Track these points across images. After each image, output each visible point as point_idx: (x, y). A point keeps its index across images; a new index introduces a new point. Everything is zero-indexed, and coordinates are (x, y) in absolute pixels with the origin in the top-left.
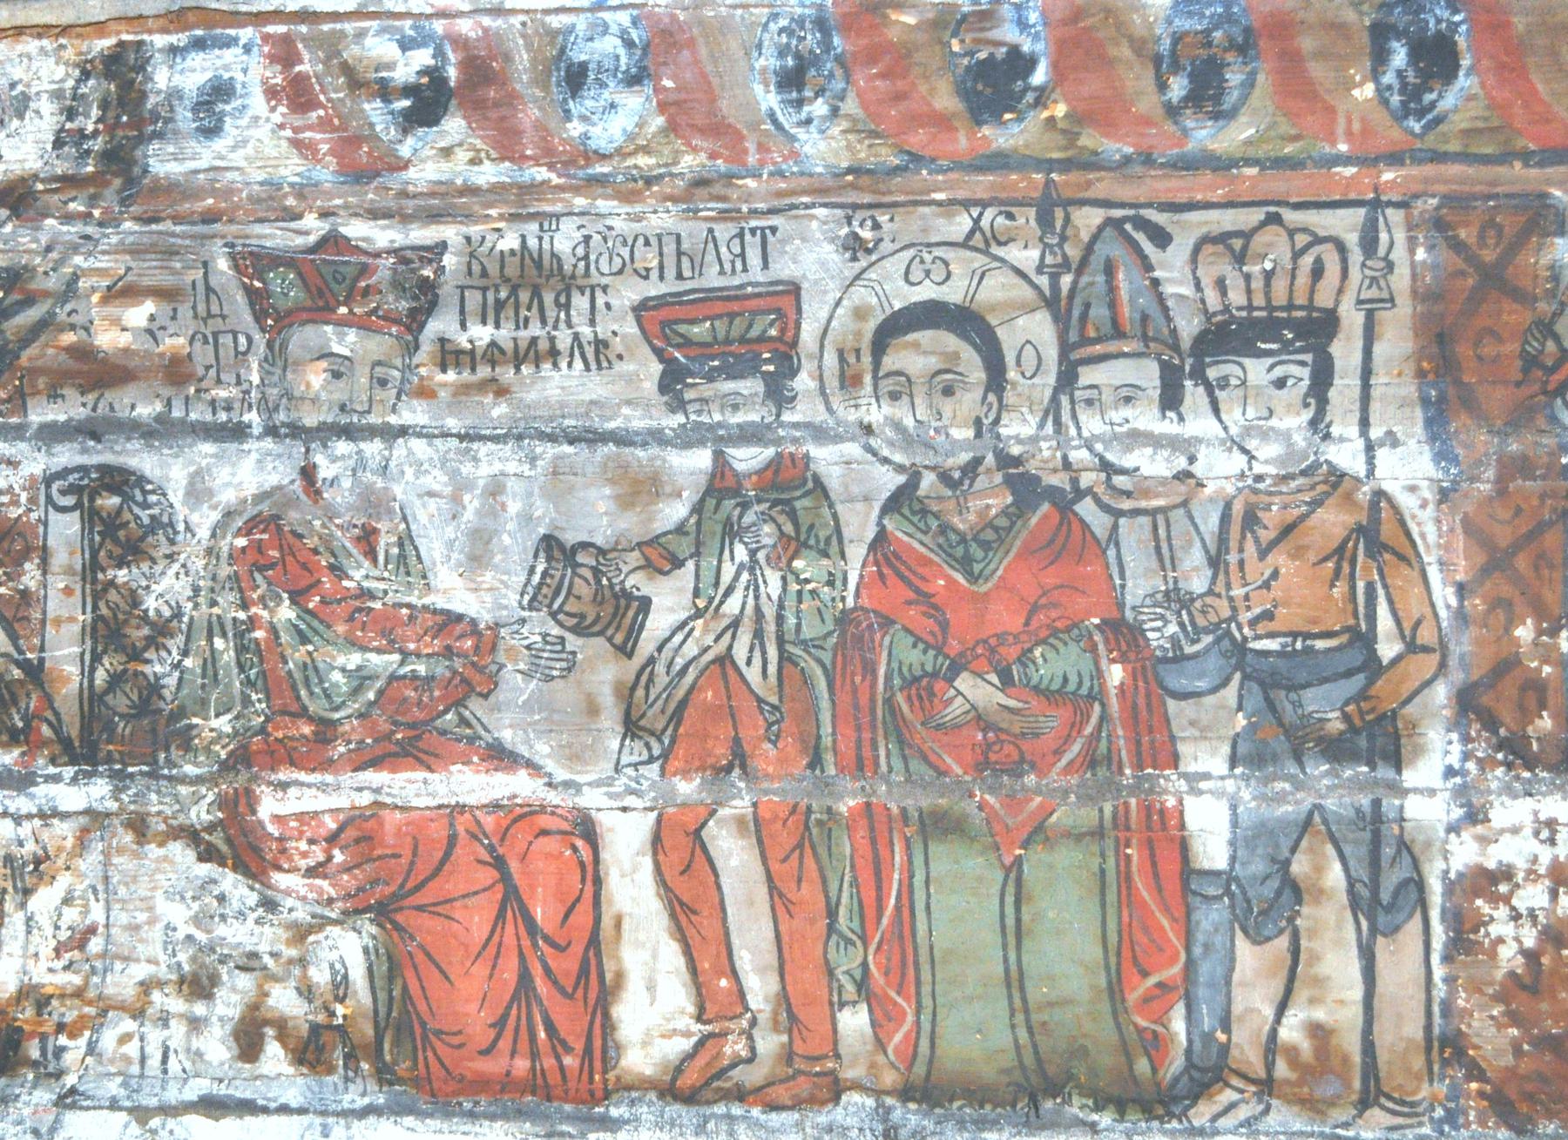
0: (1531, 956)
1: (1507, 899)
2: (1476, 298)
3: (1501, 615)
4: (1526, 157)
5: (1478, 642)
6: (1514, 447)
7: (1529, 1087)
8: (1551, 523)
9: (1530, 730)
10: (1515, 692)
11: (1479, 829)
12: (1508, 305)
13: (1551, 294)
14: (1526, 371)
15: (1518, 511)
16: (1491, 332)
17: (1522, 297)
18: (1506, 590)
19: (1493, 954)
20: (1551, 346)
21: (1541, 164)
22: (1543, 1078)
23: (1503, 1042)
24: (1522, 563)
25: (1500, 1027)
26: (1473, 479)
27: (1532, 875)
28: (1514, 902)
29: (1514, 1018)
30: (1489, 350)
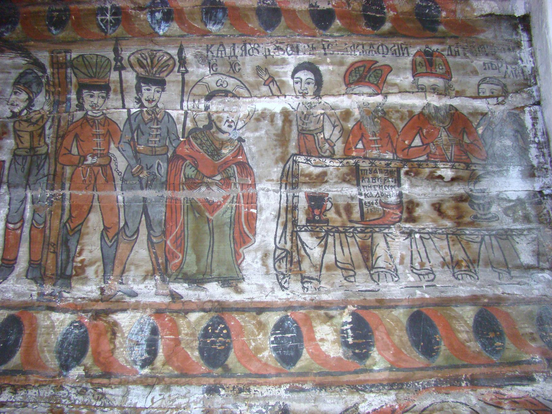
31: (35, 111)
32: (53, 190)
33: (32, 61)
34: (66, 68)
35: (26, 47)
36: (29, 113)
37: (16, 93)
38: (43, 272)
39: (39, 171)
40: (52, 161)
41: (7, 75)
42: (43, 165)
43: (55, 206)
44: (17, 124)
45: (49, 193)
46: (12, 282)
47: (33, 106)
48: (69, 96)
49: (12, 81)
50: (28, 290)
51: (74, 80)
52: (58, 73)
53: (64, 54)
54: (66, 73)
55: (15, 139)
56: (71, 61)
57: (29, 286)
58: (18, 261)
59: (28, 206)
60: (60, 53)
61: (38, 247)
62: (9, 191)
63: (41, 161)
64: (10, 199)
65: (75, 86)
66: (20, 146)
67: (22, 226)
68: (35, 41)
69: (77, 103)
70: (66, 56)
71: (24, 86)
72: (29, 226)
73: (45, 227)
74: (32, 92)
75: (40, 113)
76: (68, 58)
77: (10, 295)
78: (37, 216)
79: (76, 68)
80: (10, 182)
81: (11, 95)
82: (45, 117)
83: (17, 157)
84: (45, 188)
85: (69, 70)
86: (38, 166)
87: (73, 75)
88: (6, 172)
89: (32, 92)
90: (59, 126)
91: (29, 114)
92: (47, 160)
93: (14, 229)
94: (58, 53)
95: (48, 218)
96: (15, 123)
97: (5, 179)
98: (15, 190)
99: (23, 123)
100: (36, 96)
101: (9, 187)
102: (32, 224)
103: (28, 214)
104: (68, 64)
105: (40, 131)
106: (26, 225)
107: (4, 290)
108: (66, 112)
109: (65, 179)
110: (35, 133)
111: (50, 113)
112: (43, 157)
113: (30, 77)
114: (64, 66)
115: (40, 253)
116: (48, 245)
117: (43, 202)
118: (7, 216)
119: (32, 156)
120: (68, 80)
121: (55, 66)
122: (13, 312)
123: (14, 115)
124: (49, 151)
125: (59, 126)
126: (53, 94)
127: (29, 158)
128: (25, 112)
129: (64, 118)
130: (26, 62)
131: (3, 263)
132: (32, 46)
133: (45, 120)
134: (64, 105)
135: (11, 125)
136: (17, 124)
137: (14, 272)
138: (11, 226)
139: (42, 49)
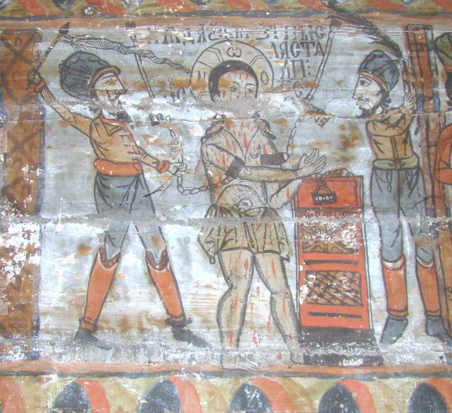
0: (18, 278)
1: (12, 258)
2: (13, 62)
3: (18, 164)
4: (30, 18)
5: (10, 173)
6: (25, 109)
7: (12, 322)
8: (36, 134)
9: (25, 201)
10: (21, 189)
11: (5, 234)
12: (23, 64)
13: (37, 60)
14: (29, 85)
15: (26, 130)
16: (18, 72)
17: (27, 61)
18: (20, 155)
19: (5, 277)
20: (37, 77)
21: (35, 20)
22: (16, 319)
23: (6, 307)
24: (26, 147)
25: (5, 302)
26: (11, 120)
27: (21, 250)
28: (14, 259)
29: (10, 299)
30: (18, 78)
31: (392, 109)
32: (435, 216)
33: (381, 39)
34: (429, 50)
35: (370, 20)
36: (385, 111)
37: (363, 83)
38: (446, 326)
39: (412, 190)
40: (427, 177)
41: (348, 57)
42: (416, 183)
43: (443, 239)
44: (370, 126)
45: (431, 221)
46: (409, 340)
47: (389, 101)
48: (435, 90)
49: (357, 66)
50: (432, 350)
51: (440, 68)
52: (418, 57)
53: (422, 31)
54: (429, 57)
55: (372, 147)
56: (434, 41)
57: (433, 344)
58: (409, 311)
59: (407, 238)
60: (418, 29)
61: (432, 293)
62: (376, 216)
63: (412, 178)
64: (380, 227)
65: (443, 76)
66: (380, 156)
67: (404, 263)
68: (382, 11)
69: (448, 99)
70: (426, 34)
71: (373, 73)
72: (413, 265)
73: (434, 266)
74: (385, 83)
75: (400, 112)
76: (430, 37)
77: (409, 357)
78: (420, 252)
79: (441, 51)
80: (375, 205)
81: (356, 86)
82: (408, 117)
83: (379, 172)
84: (424, 214)
85: (432, 54)
86: (409, 184)
87: (438, 61)
88: (367, 193)
89: (385, 83)
90: (428, 129)
91: (386, 113)
92: (420, 177)
93: (394, 269)
94: (414, 30)
95: (437, 254)
96: (367, 123)
97: (367, 201)
98: (385, 217)
99: (379, 125)
100: (391, 88)
101: (375, 212)
102: (417, 262)
103: (409, 249)
104: (431, 46)
105: (404, 136)
106: (408, 263)
107: (400, 350)
108: (435, 112)
109: (449, 202)
110: (397, 138)
111: (414, 112)
112: (414, 171)
113: (380, 62)
114: (425, 48)
115: (437, 300)
116: (445, 289)
117: (427, 233)
118: (381, 250)
119: (399, 170)
120: (433, 68)
121: (413, 48)
122: (423, 380)
123: (366, 114)
124: (421, 164)
125: (428, 129)
126: (414, 86)
127: (395, 173)
128: (379, 110)
129: (434, 120)
130: (372, 41)
131: (390, 314)
132: (377, 18)
133: (408, 122)
134: (431, 102)
135: (362, 127)
136: (370, 126)
137: (409, 326)
138: (389, 265)
139: (391, 23)
